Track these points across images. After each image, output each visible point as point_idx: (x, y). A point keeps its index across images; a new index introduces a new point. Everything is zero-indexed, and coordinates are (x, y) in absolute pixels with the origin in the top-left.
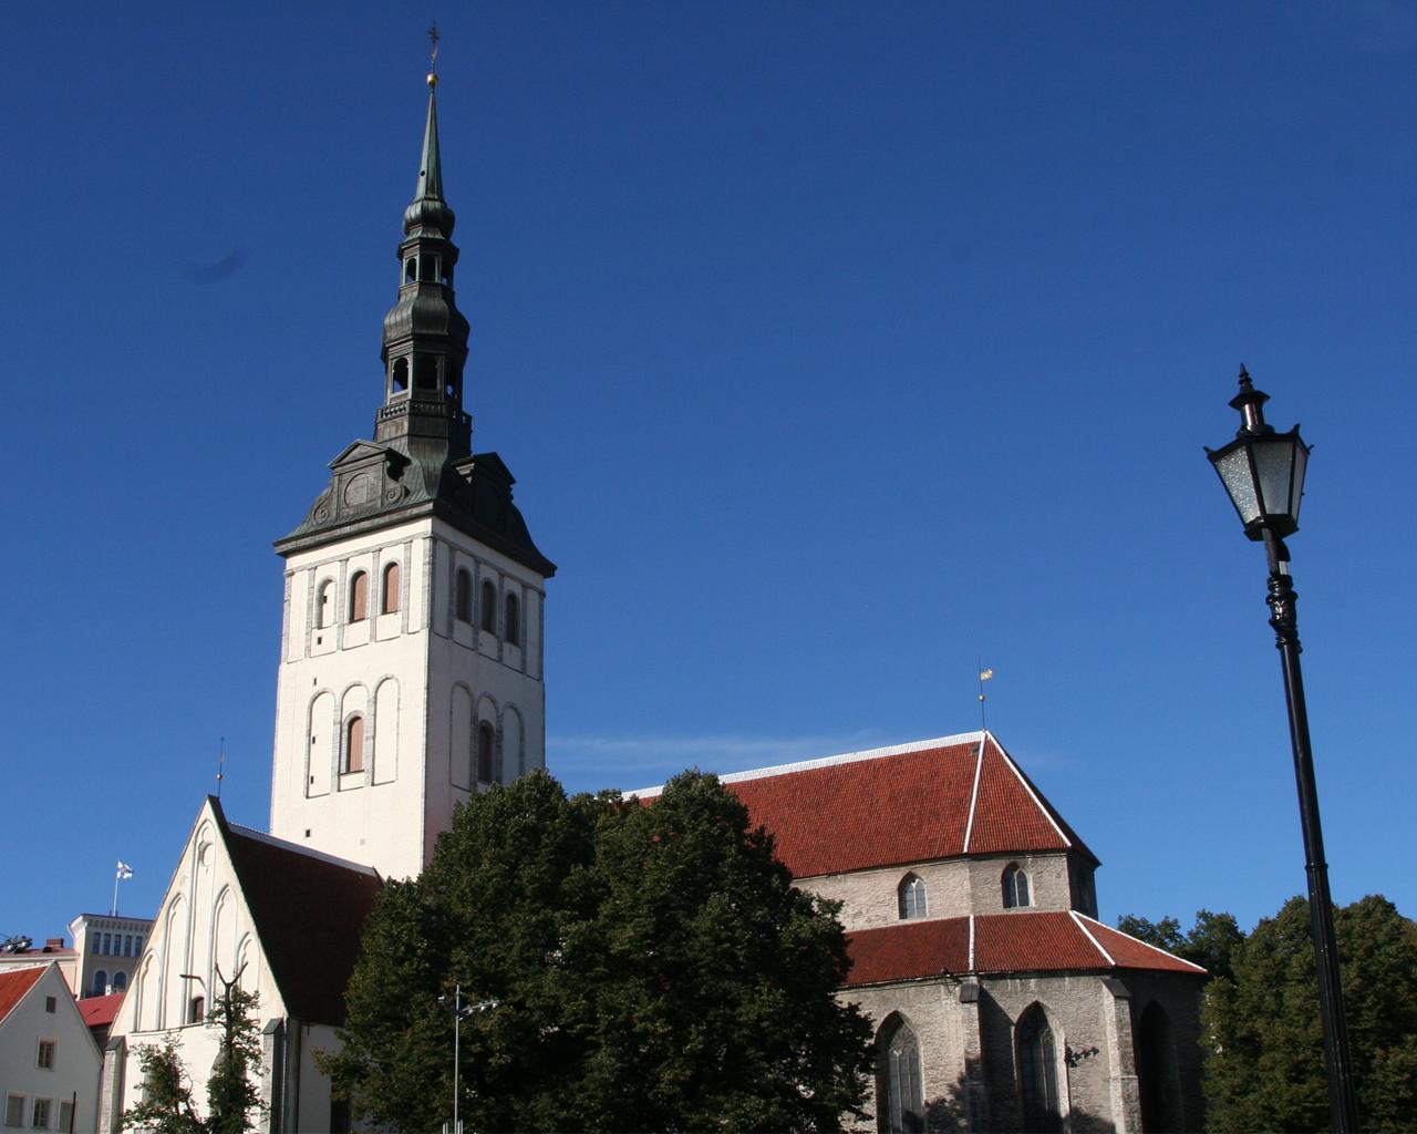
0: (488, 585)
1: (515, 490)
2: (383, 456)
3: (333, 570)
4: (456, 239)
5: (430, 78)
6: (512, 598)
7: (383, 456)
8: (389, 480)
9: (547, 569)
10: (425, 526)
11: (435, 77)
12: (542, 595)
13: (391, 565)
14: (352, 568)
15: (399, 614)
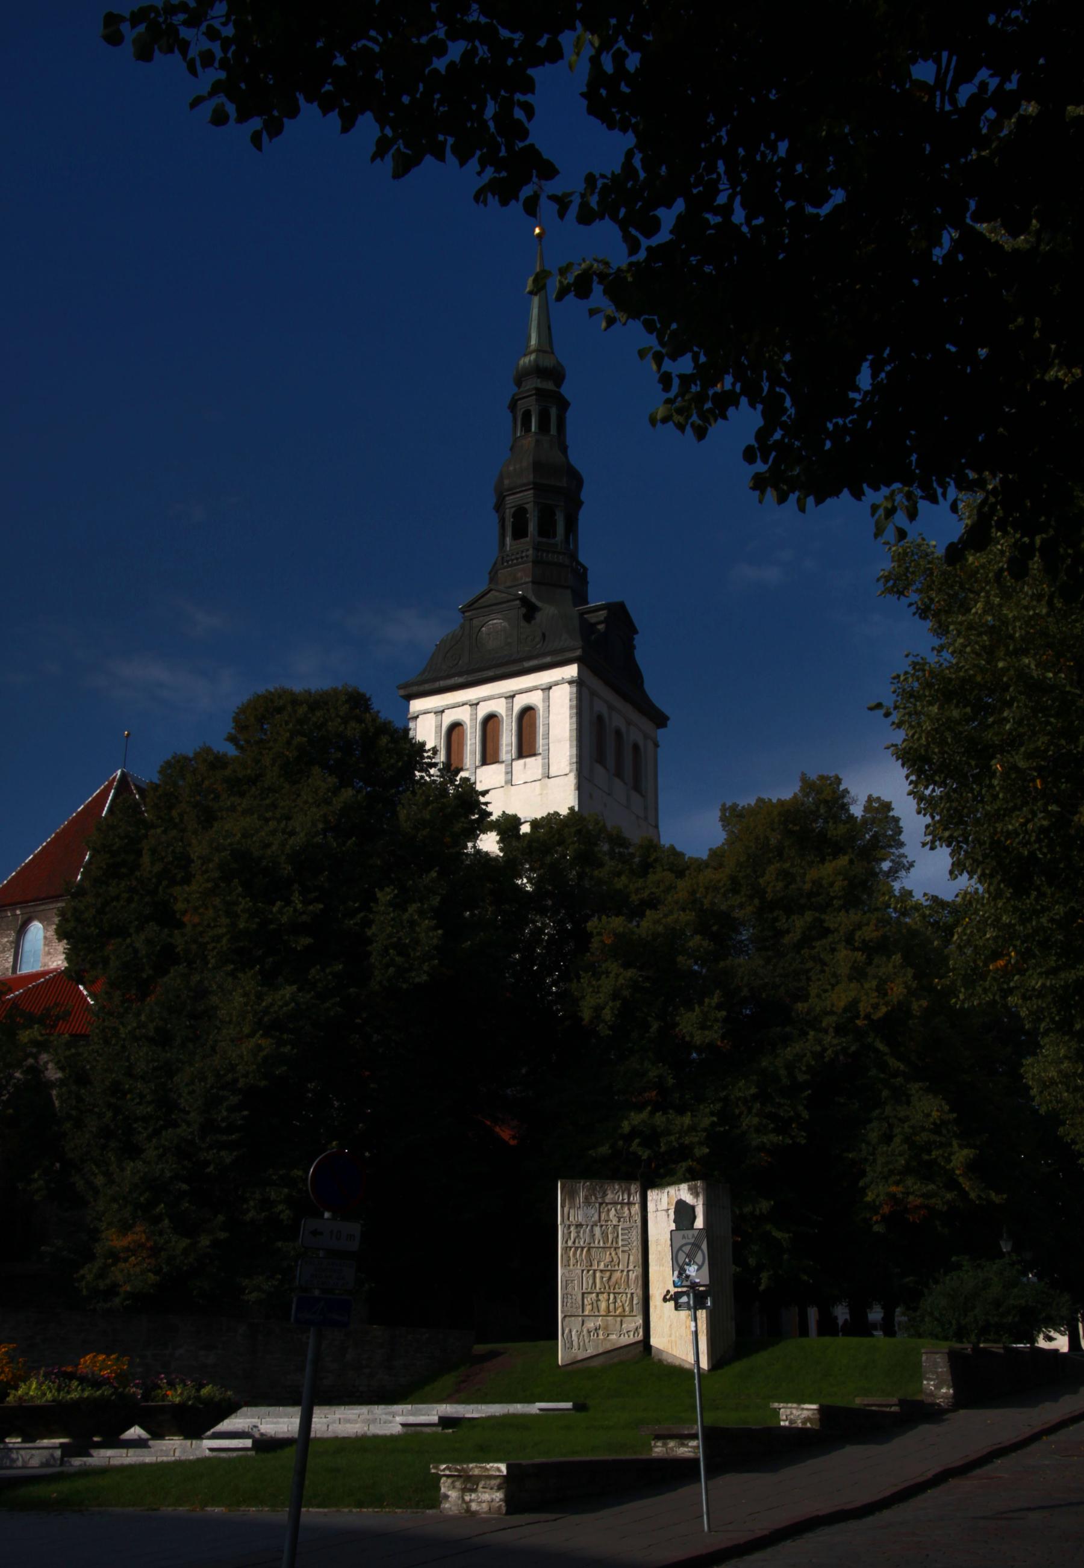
0: (618, 733)
1: (638, 640)
2: (518, 602)
3: (462, 715)
4: (566, 390)
5: (537, 231)
6: (636, 747)
7: (518, 602)
8: (523, 624)
9: (660, 720)
10: (571, 671)
11: (542, 229)
12: (656, 745)
13: (528, 711)
14: (483, 711)
15: (539, 758)
